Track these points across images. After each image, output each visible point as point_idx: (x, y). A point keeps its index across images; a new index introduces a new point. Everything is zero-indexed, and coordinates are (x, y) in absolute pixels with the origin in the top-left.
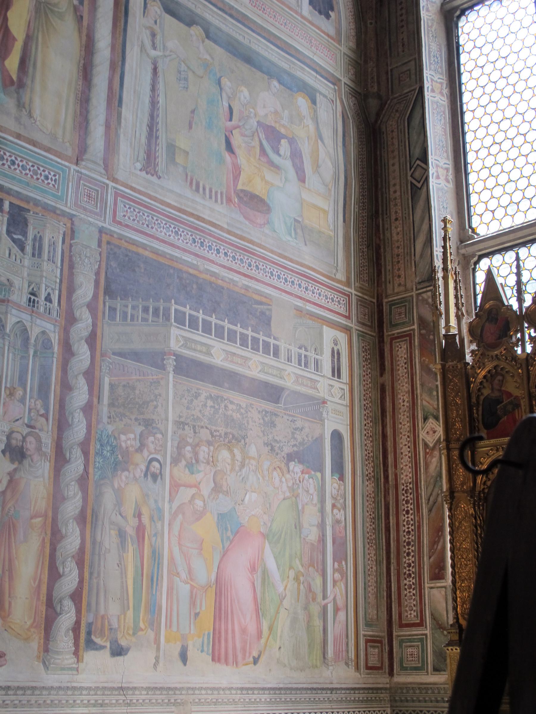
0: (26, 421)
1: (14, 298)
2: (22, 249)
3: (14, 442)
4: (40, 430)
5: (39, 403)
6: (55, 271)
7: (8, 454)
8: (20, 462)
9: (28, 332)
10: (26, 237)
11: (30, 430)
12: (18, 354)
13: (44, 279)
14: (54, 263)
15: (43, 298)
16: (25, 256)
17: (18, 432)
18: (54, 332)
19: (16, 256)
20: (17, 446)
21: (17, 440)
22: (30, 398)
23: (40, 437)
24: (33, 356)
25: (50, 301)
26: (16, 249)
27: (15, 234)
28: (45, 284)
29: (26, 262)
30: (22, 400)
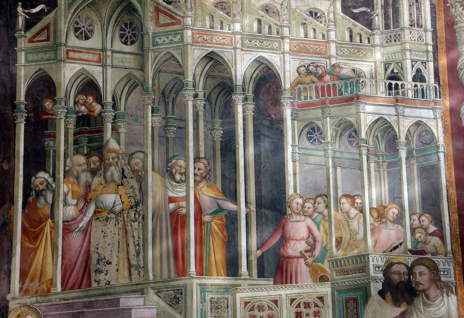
0: (409, 246)
1: (366, 91)
2: (369, 24)
3: (396, 278)
4: (432, 254)
5: (426, 220)
6: (424, 38)
7: (388, 295)
8: (410, 303)
9: (393, 129)
10: (373, 6)
11: (417, 257)
12: (384, 162)
13: (408, 53)
14: (421, 27)
15: (410, 77)
16: (374, 32)
17: (399, 263)
18: (435, 118)
19: (361, 36)
20: (401, 282)
21: (399, 273)
22: (411, 215)
23: (434, 262)
24: (407, 159)
25: (422, 79)
26: (359, 27)
27: (356, 8)
28: (411, 59)
29: (377, 39)
30: (399, 220)
